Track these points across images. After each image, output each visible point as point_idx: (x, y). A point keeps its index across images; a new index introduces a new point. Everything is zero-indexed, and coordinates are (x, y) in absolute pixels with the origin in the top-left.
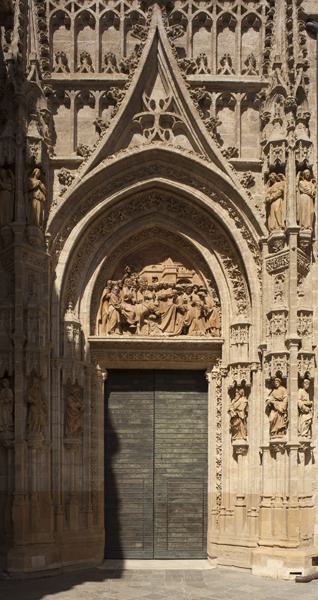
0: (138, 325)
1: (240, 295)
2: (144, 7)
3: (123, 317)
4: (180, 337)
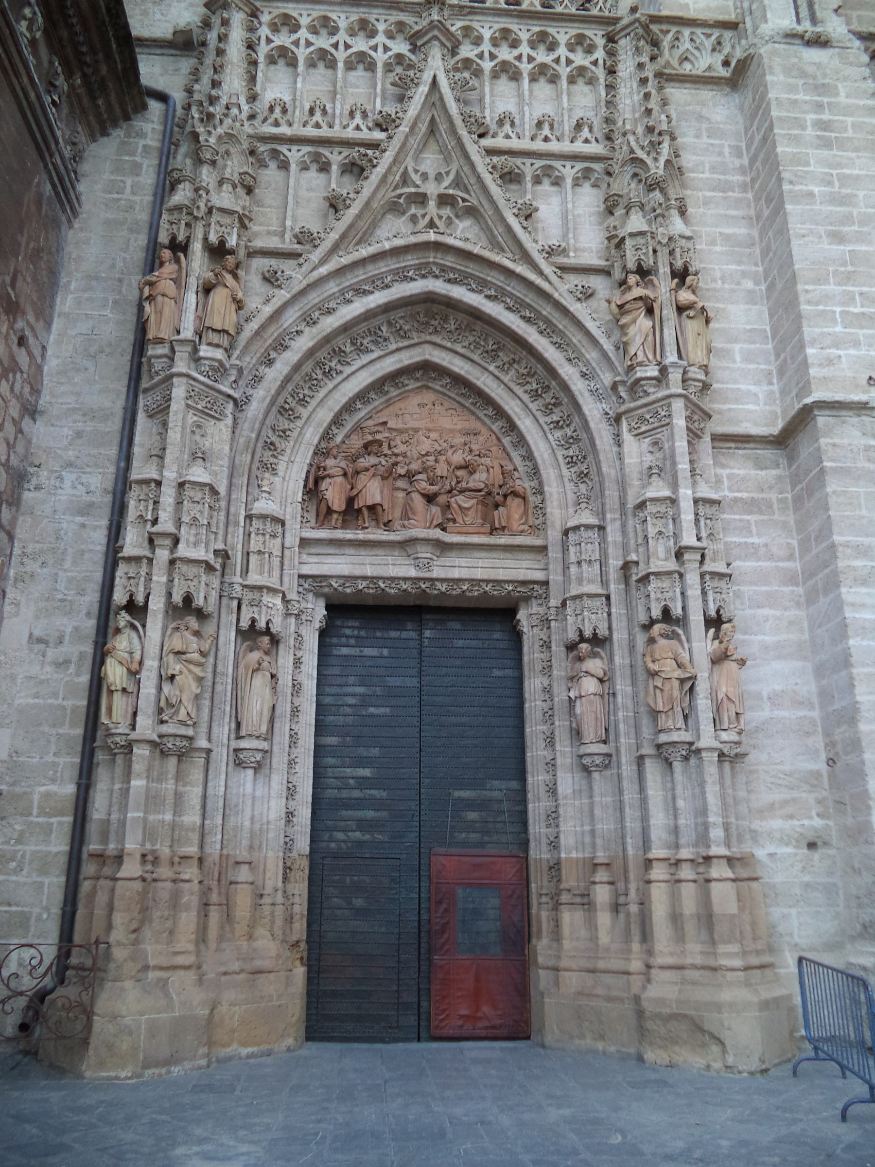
2: (414, 49)
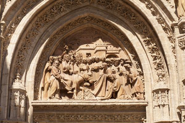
0: (75, 91)
1: (159, 66)
3: (62, 85)
4: (110, 100)
